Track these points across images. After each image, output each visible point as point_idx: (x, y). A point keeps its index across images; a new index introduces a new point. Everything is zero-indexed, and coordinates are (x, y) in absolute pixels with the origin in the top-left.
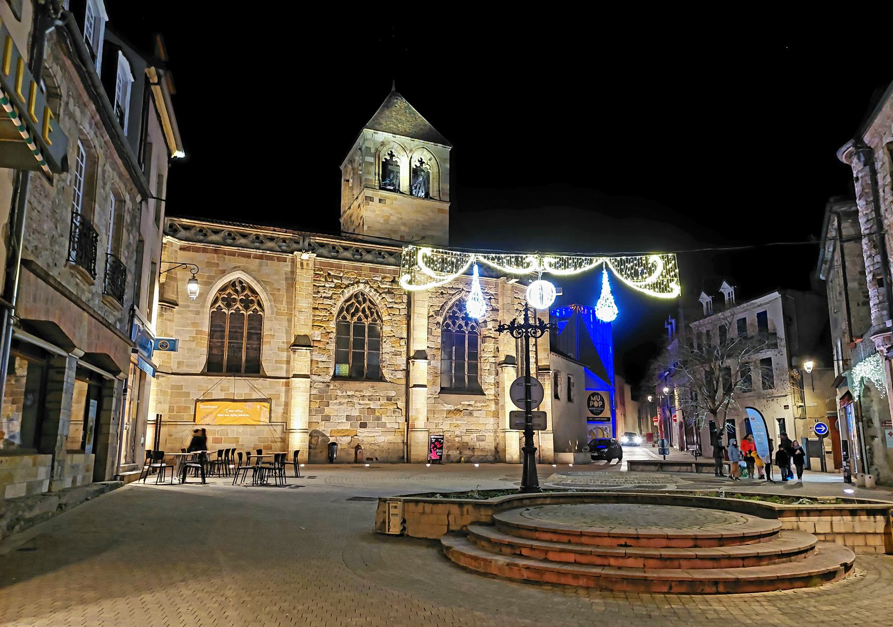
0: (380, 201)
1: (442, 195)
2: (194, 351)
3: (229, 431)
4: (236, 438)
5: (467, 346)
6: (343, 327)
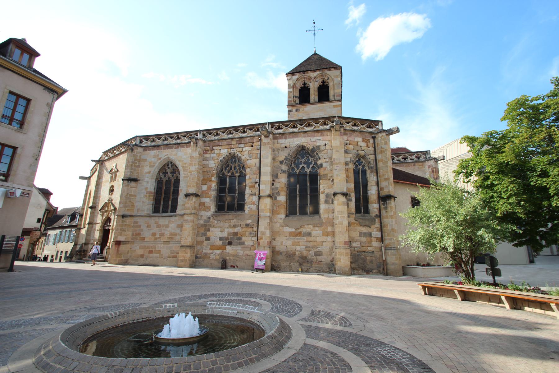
0: (296, 110)
1: (336, 97)
3: (156, 246)
4: (160, 251)
5: (308, 184)
6: (221, 181)
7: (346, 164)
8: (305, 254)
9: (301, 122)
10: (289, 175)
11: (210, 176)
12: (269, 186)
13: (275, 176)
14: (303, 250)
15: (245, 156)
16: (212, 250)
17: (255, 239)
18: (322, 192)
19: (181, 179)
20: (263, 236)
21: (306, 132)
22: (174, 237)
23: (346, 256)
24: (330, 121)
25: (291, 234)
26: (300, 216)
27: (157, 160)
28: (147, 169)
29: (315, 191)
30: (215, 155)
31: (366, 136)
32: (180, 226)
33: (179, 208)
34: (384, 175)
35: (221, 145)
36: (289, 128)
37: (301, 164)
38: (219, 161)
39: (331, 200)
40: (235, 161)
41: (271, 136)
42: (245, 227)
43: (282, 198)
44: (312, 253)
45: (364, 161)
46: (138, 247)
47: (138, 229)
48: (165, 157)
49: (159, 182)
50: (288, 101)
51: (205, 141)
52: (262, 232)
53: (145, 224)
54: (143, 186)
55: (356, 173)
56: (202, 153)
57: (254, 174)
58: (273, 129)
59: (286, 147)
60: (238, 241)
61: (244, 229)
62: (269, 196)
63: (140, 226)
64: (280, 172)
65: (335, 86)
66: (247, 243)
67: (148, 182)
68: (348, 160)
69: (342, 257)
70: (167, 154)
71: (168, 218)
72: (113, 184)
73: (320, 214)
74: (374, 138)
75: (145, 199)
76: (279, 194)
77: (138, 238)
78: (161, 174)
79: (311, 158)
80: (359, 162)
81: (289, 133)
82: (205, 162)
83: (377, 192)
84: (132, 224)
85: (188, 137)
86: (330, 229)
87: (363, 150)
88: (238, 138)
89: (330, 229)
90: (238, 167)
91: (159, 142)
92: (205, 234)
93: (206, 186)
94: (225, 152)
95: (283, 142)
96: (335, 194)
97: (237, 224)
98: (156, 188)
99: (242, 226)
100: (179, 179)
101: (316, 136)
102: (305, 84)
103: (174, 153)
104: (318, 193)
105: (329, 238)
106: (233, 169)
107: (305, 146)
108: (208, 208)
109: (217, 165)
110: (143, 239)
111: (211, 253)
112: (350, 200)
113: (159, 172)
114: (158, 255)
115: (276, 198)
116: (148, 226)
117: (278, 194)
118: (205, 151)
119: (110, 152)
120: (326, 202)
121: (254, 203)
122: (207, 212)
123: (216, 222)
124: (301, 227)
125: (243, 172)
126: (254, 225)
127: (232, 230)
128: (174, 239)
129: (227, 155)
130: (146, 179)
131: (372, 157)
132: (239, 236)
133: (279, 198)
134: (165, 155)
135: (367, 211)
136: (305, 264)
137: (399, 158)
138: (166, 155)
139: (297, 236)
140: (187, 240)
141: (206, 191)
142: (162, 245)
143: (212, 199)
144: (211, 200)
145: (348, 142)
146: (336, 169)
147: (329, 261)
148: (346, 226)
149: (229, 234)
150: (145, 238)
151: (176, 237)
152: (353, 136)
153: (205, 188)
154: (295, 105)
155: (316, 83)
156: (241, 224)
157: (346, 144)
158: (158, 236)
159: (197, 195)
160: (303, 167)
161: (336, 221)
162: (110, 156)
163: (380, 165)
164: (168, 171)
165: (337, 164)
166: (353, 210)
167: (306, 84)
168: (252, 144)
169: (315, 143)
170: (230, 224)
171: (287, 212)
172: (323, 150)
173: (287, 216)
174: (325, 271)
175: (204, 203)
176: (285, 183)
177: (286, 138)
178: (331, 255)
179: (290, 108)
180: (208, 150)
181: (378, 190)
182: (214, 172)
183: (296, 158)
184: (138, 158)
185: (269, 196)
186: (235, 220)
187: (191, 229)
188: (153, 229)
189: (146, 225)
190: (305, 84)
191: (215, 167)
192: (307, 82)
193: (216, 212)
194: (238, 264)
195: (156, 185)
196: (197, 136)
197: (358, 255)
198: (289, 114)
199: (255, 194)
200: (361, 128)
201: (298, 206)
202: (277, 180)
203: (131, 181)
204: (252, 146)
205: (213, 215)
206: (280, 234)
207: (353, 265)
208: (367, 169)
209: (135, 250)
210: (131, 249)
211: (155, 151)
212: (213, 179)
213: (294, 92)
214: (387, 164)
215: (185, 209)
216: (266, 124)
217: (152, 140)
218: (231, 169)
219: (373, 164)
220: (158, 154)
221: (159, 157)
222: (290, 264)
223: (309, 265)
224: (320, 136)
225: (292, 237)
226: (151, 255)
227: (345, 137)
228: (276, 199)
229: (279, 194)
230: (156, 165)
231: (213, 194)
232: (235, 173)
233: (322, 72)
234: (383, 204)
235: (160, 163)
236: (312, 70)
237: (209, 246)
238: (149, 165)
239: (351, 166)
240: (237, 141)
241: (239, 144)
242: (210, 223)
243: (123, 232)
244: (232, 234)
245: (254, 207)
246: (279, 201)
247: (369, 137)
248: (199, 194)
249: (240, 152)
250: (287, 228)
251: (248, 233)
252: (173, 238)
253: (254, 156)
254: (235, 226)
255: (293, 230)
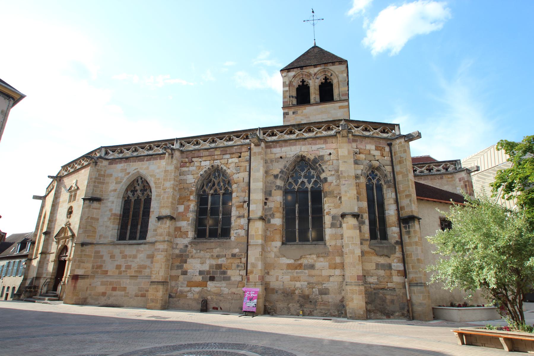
0: (294, 113)
1: (342, 96)
2: (108, 227)
4: (125, 287)
5: (310, 203)
6: (202, 200)
7: (357, 177)
8: (307, 292)
9: (300, 127)
10: (286, 192)
11: (188, 194)
12: (260, 206)
13: (268, 194)
14: (304, 286)
15: (231, 169)
16: (189, 287)
17: (243, 273)
18: (327, 213)
19: (153, 198)
20: (254, 269)
21: (305, 139)
22: (143, 270)
23: (359, 295)
24: (335, 125)
25: (289, 266)
26: (300, 243)
27: (125, 176)
28: (112, 186)
29: (319, 212)
30: (194, 168)
31: (380, 142)
32: (151, 257)
33: (150, 234)
34: (404, 191)
35: (202, 157)
36: (285, 134)
37: (300, 178)
38: (199, 175)
39: (338, 223)
40: (219, 175)
41: (263, 144)
42: (230, 258)
43: (278, 221)
44: (316, 290)
45: (378, 174)
46: (99, 283)
47: (100, 260)
48: (134, 172)
49: (127, 202)
50: (284, 102)
51: (182, 152)
52: (251, 263)
53: (108, 254)
54: (107, 207)
55: (369, 188)
56: (179, 165)
57: (243, 191)
58: (265, 136)
59: (281, 158)
60: (222, 276)
61: (229, 261)
62: (262, 219)
63: (102, 257)
64: (275, 188)
65: (341, 83)
66: (233, 279)
67: (113, 202)
68: (359, 172)
69: (354, 296)
70: (137, 167)
71: (135, 246)
72: (72, 204)
73: (325, 241)
74: (390, 145)
75: (109, 223)
76: (273, 216)
77: (100, 272)
78: (129, 192)
79: (312, 171)
80: (373, 175)
81: (286, 141)
82: (182, 177)
83: (396, 212)
84: (93, 254)
85: (162, 147)
86: (338, 260)
87: (378, 160)
88: (222, 147)
89: (338, 260)
90: (223, 182)
91: (128, 154)
92: (180, 267)
93: (183, 206)
94: (206, 164)
95: (278, 151)
96: (343, 216)
97: (221, 253)
98: (122, 209)
99: (227, 256)
100: (151, 199)
101: (319, 144)
102: (303, 81)
103: (145, 166)
104: (322, 214)
105: (338, 272)
106: (216, 185)
107: (304, 157)
108: (185, 234)
109: (196, 180)
110: (106, 272)
111: (188, 291)
112: (363, 223)
113: (127, 190)
114: (123, 293)
115: (269, 221)
116: (112, 257)
117: (272, 216)
118: (182, 164)
119: (70, 167)
120: (333, 225)
121: (242, 228)
122: (184, 238)
123: (194, 251)
124: (301, 257)
125: (229, 188)
126: (242, 255)
127: (214, 262)
128: (143, 273)
129: (209, 168)
130: (111, 199)
131: (388, 169)
132: (224, 269)
133: (273, 221)
134: (134, 169)
135: (384, 236)
136: (307, 306)
137: (423, 169)
138: (135, 169)
139: (296, 268)
140: (159, 274)
141: (183, 212)
142: (128, 281)
143: (190, 222)
144: (189, 224)
145: (358, 150)
146: (344, 184)
147: (338, 301)
148: (359, 256)
149: (211, 266)
150: (107, 271)
151: (145, 270)
152: (364, 143)
153: (181, 208)
154: (292, 107)
155: (317, 80)
156: (226, 254)
157: (356, 153)
158: (123, 269)
159: (172, 218)
160: (303, 182)
161: (345, 250)
162: (69, 171)
163: (399, 178)
164: (138, 188)
165: (345, 177)
166: (367, 235)
167: (305, 81)
168: (239, 154)
169: (317, 152)
170: (212, 254)
171: (284, 239)
172: (327, 161)
173: (283, 244)
174: (334, 314)
175: (180, 228)
176: (281, 202)
177: (281, 147)
178: (340, 293)
179: (286, 111)
180: (186, 163)
181: (398, 210)
182: (193, 189)
183: (295, 170)
184: (102, 173)
185: (262, 219)
186: (218, 249)
187: (164, 260)
188: (118, 260)
189: (110, 255)
190: (303, 81)
191: (194, 182)
192: (306, 79)
193: (195, 238)
194: (222, 305)
195: (123, 205)
196: (173, 145)
197: (375, 293)
198: (284, 117)
199: (244, 217)
200: (374, 133)
201: (297, 231)
202: (271, 199)
203: (93, 202)
204: (240, 157)
205: (191, 243)
206: (275, 267)
207: (369, 307)
208: (383, 183)
209: (95, 287)
210: (90, 285)
211: (122, 165)
212: (192, 197)
213: (290, 91)
214: (408, 177)
215: (157, 236)
216: (256, 129)
217: (119, 151)
218: (214, 185)
219: (390, 177)
220: (125, 168)
221: (127, 171)
222: (288, 305)
223: (312, 306)
224: (323, 143)
225: (290, 271)
226: (114, 293)
227: (354, 145)
228: (270, 222)
229: (274, 216)
230: (124, 181)
231: (191, 216)
232: (218, 190)
233: (324, 68)
234: (405, 227)
235: (128, 178)
236: (312, 65)
237: (186, 282)
238: (115, 182)
239: (363, 180)
240: (221, 151)
241: (223, 154)
242: (187, 253)
243: (82, 264)
244: (214, 267)
245: (242, 233)
246: (273, 224)
247: (383, 144)
248: (175, 216)
249: (225, 165)
250: (284, 258)
251: (234, 266)
252: (142, 271)
253: (242, 169)
254: (218, 257)
255: (291, 261)
